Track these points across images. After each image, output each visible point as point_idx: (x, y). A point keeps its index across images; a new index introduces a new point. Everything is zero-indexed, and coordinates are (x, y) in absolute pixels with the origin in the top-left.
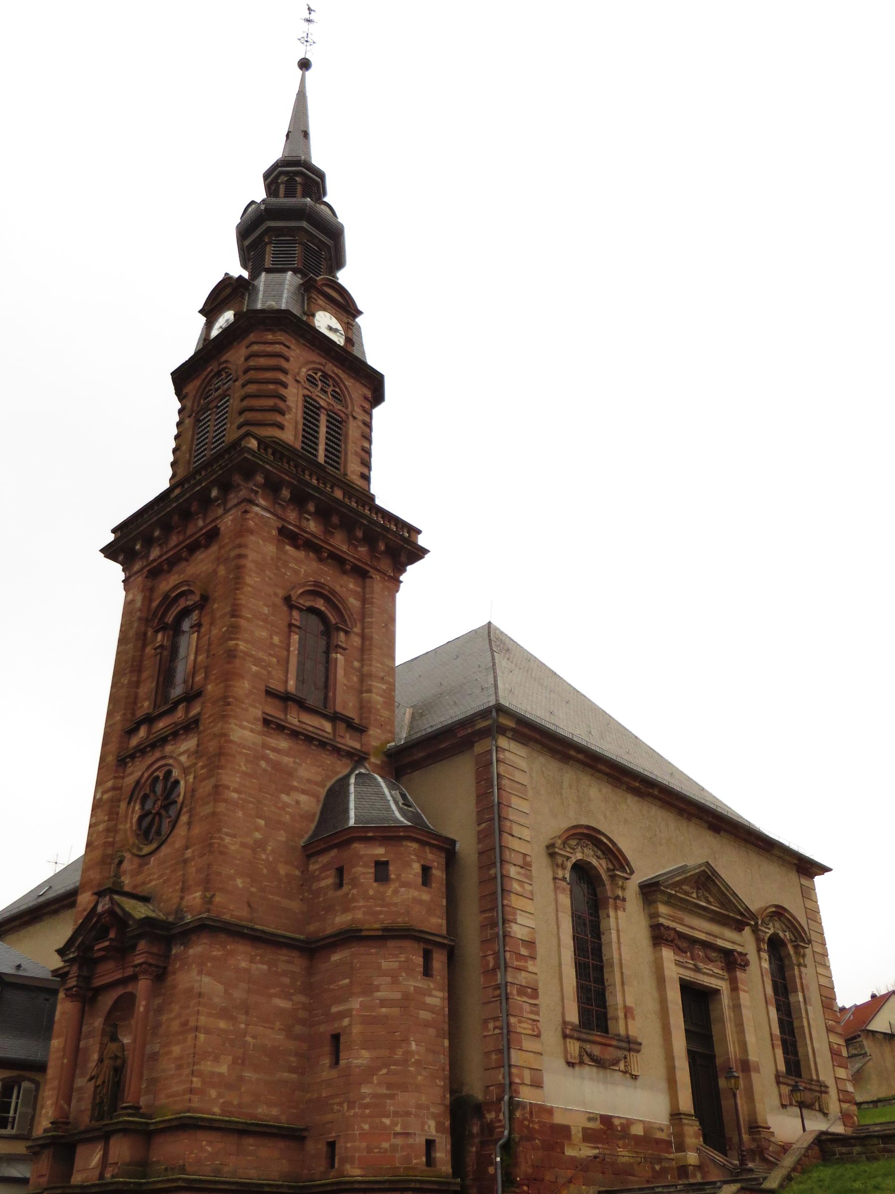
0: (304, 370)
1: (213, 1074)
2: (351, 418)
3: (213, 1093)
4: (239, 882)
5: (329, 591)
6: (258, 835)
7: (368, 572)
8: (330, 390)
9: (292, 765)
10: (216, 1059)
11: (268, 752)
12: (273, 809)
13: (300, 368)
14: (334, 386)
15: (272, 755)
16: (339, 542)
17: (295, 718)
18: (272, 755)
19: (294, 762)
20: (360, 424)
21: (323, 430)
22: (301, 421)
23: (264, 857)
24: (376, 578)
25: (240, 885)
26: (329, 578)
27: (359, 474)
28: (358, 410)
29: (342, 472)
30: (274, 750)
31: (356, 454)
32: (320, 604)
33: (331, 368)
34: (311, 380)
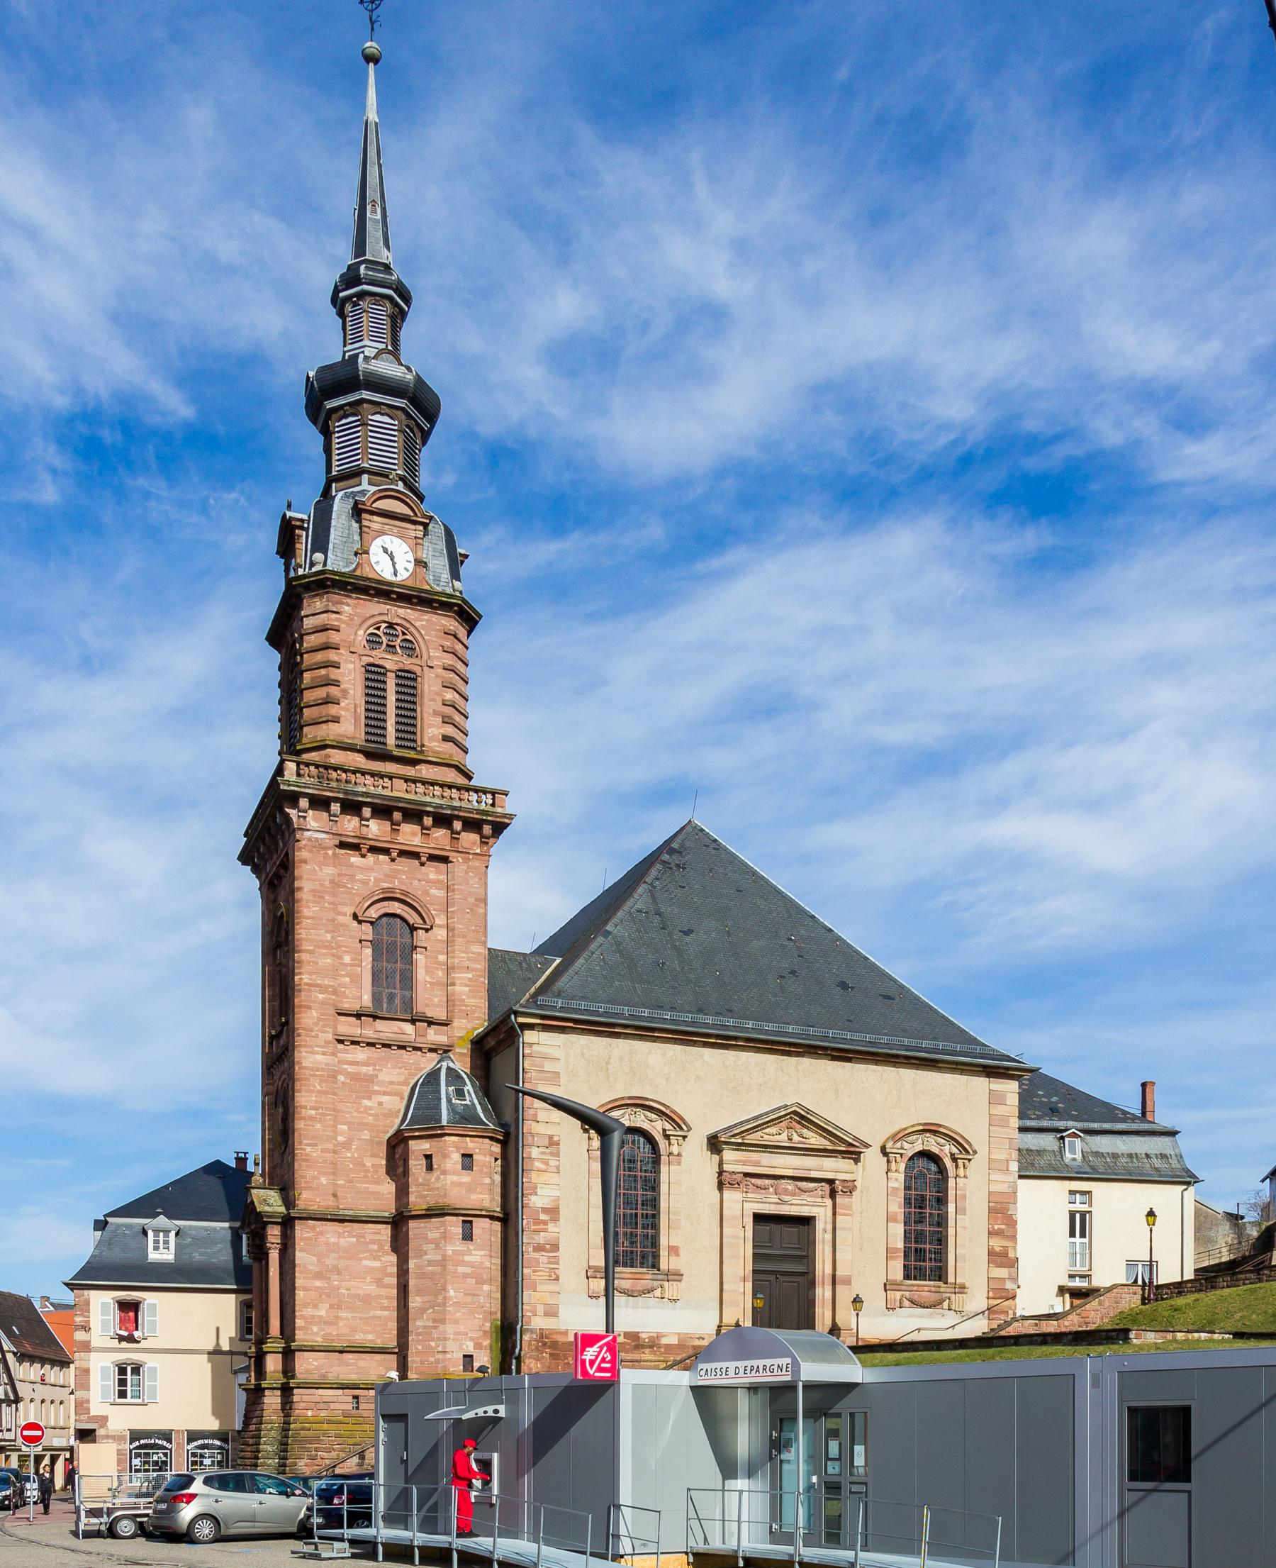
0: (361, 632)
1: (313, 1316)
2: (426, 669)
3: (315, 1329)
4: (323, 1180)
5: (401, 894)
6: (341, 1139)
7: (448, 857)
8: (398, 642)
9: (372, 1073)
10: (316, 1306)
11: (346, 1066)
12: (355, 1114)
13: (356, 633)
14: (404, 634)
15: (350, 1069)
16: (410, 835)
17: (370, 1030)
18: (350, 1069)
19: (374, 1070)
20: (440, 671)
21: (391, 698)
22: (361, 701)
23: (349, 1155)
24: (458, 861)
25: (325, 1183)
26: (404, 877)
27: (440, 737)
28: (436, 654)
29: (419, 744)
30: (352, 1063)
31: (435, 713)
32: (396, 908)
33: (401, 613)
34: (373, 641)
